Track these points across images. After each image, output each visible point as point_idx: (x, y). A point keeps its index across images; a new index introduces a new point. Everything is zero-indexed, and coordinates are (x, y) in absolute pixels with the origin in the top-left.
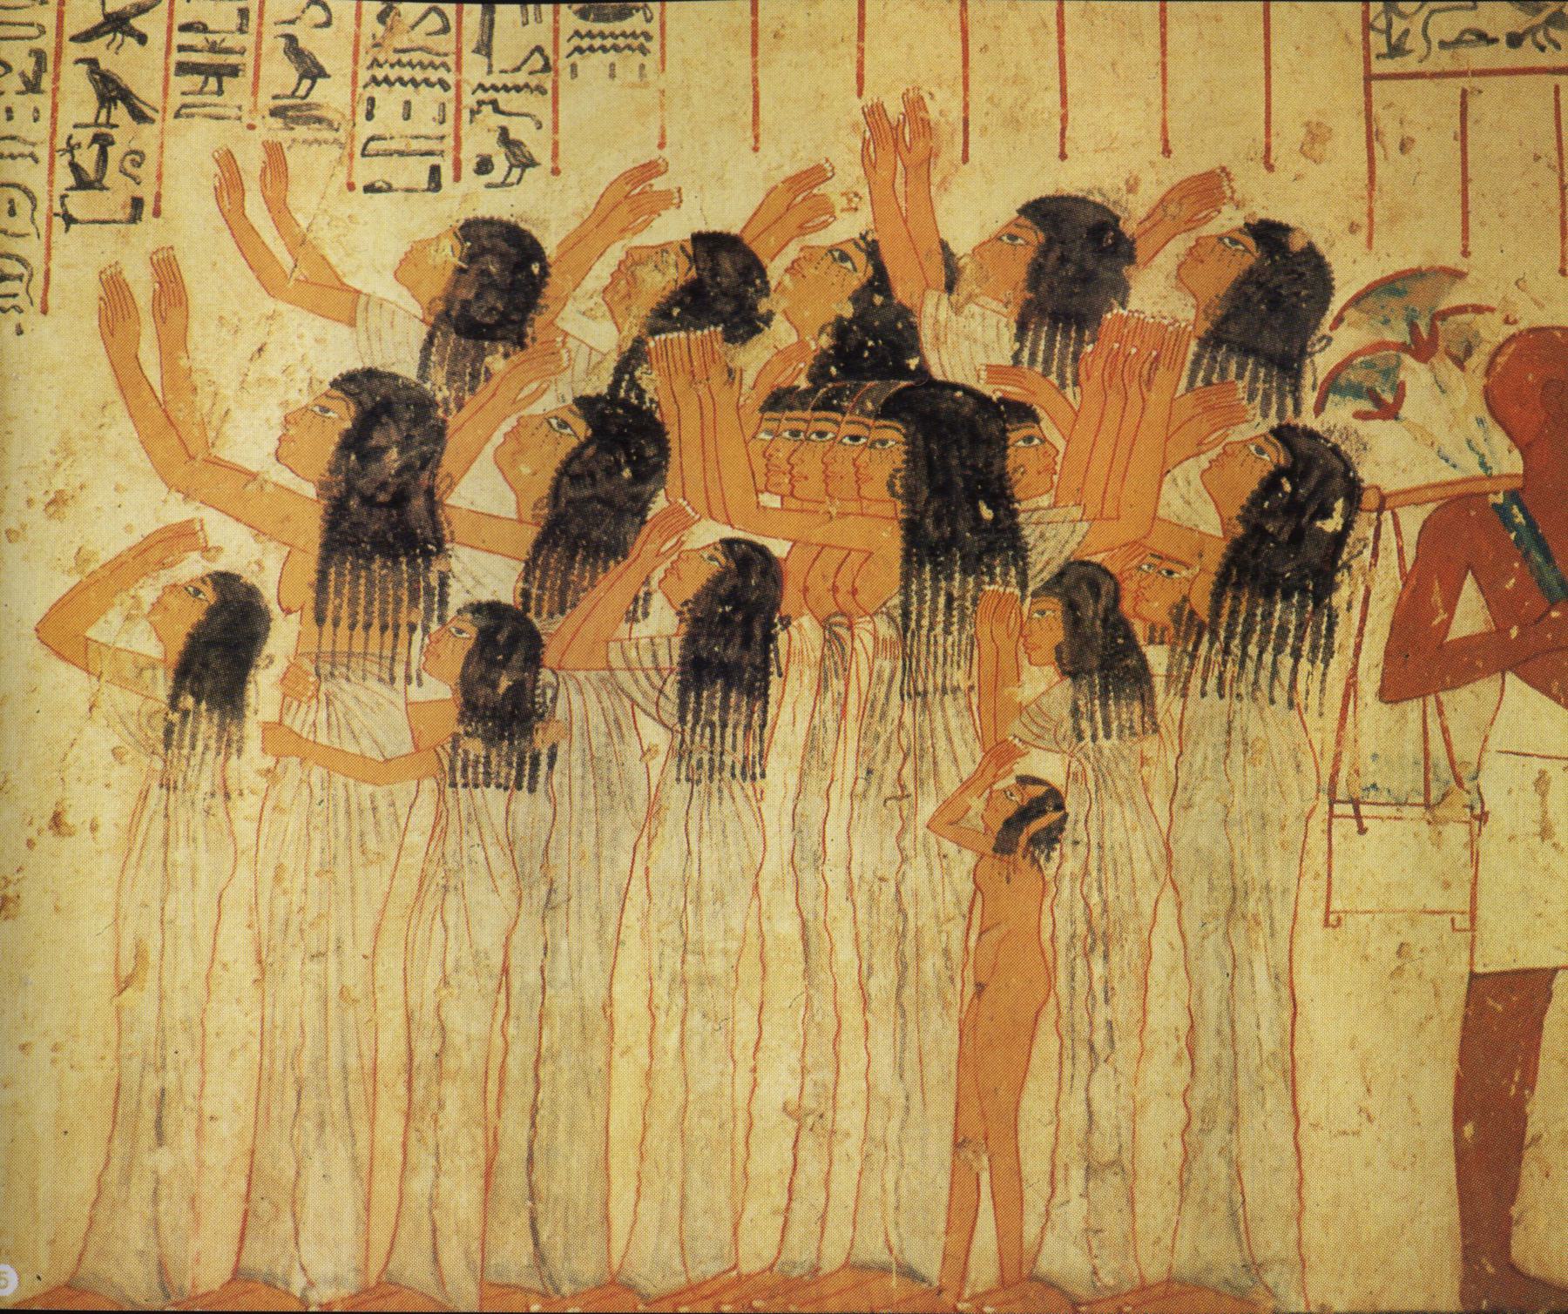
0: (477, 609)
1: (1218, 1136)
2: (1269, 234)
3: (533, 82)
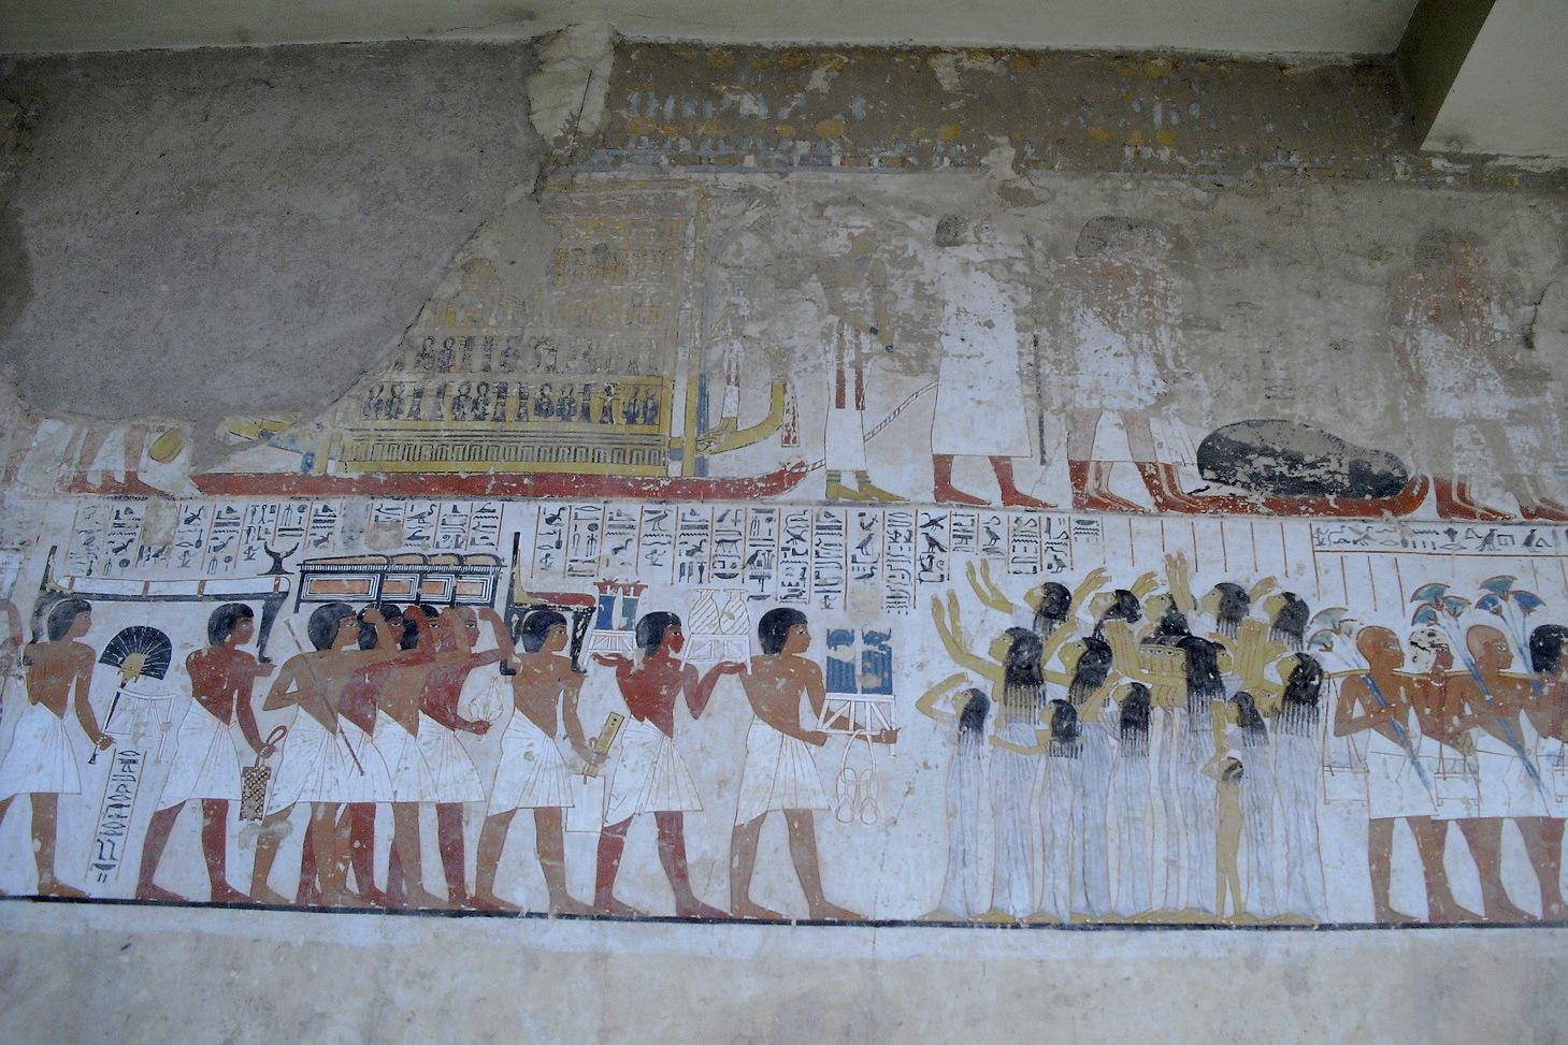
0: (1055, 701)
1: (1298, 869)
2: (1289, 596)
3: (1064, 541)
